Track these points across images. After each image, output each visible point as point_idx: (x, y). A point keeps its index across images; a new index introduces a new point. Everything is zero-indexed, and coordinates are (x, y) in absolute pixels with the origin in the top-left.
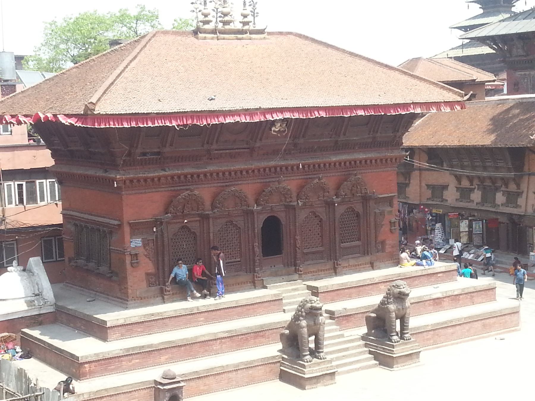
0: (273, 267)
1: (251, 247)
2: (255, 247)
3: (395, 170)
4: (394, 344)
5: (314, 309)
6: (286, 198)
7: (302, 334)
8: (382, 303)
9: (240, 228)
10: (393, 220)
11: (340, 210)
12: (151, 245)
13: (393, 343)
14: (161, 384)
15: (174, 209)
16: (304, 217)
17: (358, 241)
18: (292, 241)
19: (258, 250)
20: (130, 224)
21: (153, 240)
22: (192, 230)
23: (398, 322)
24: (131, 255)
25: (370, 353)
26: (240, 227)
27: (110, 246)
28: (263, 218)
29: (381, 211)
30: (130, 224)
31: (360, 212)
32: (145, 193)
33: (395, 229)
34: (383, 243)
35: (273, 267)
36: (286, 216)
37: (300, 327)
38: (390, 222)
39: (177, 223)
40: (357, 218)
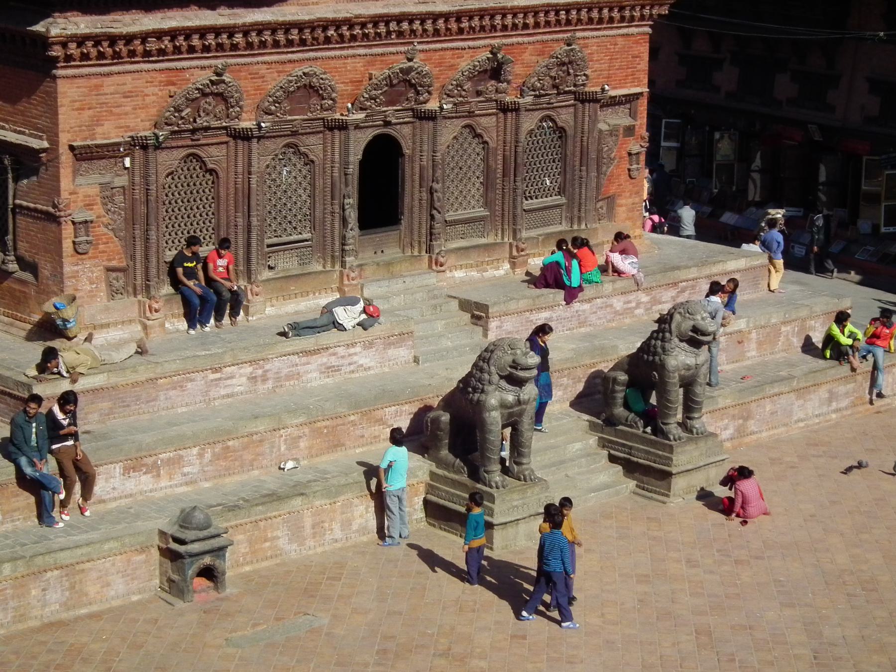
0: (379, 253)
1: (337, 209)
2: (347, 207)
3: (644, 34)
4: (673, 443)
5: (521, 369)
6: (418, 93)
7: (489, 421)
8: (646, 348)
9: (313, 162)
10: (635, 149)
11: (529, 122)
12: (119, 198)
13: (670, 440)
14: (177, 540)
15: (175, 117)
16: (452, 137)
17: (560, 194)
18: (424, 194)
19: (353, 215)
20: (72, 148)
21: (123, 187)
22: (210, 166)
23: (681, 391)
24: (74, 223)
25: (613, 459)
26: (315, 159)
27: (14, 198)
28: (366, 136)
29: (611, 128)
30: (72, 148)
31: (567, 129)
32: (109, 74)
33: (638, 169)
34: (611, 200)
35: (379, 253)
36: (414, 135)
37: (479, 407)
38: (630, 154)
39: (182, 147)
40: (559, 143)
